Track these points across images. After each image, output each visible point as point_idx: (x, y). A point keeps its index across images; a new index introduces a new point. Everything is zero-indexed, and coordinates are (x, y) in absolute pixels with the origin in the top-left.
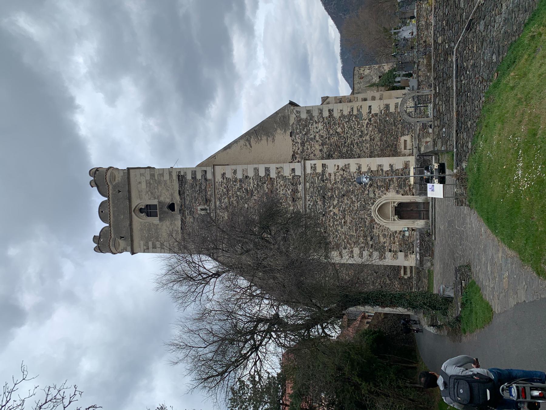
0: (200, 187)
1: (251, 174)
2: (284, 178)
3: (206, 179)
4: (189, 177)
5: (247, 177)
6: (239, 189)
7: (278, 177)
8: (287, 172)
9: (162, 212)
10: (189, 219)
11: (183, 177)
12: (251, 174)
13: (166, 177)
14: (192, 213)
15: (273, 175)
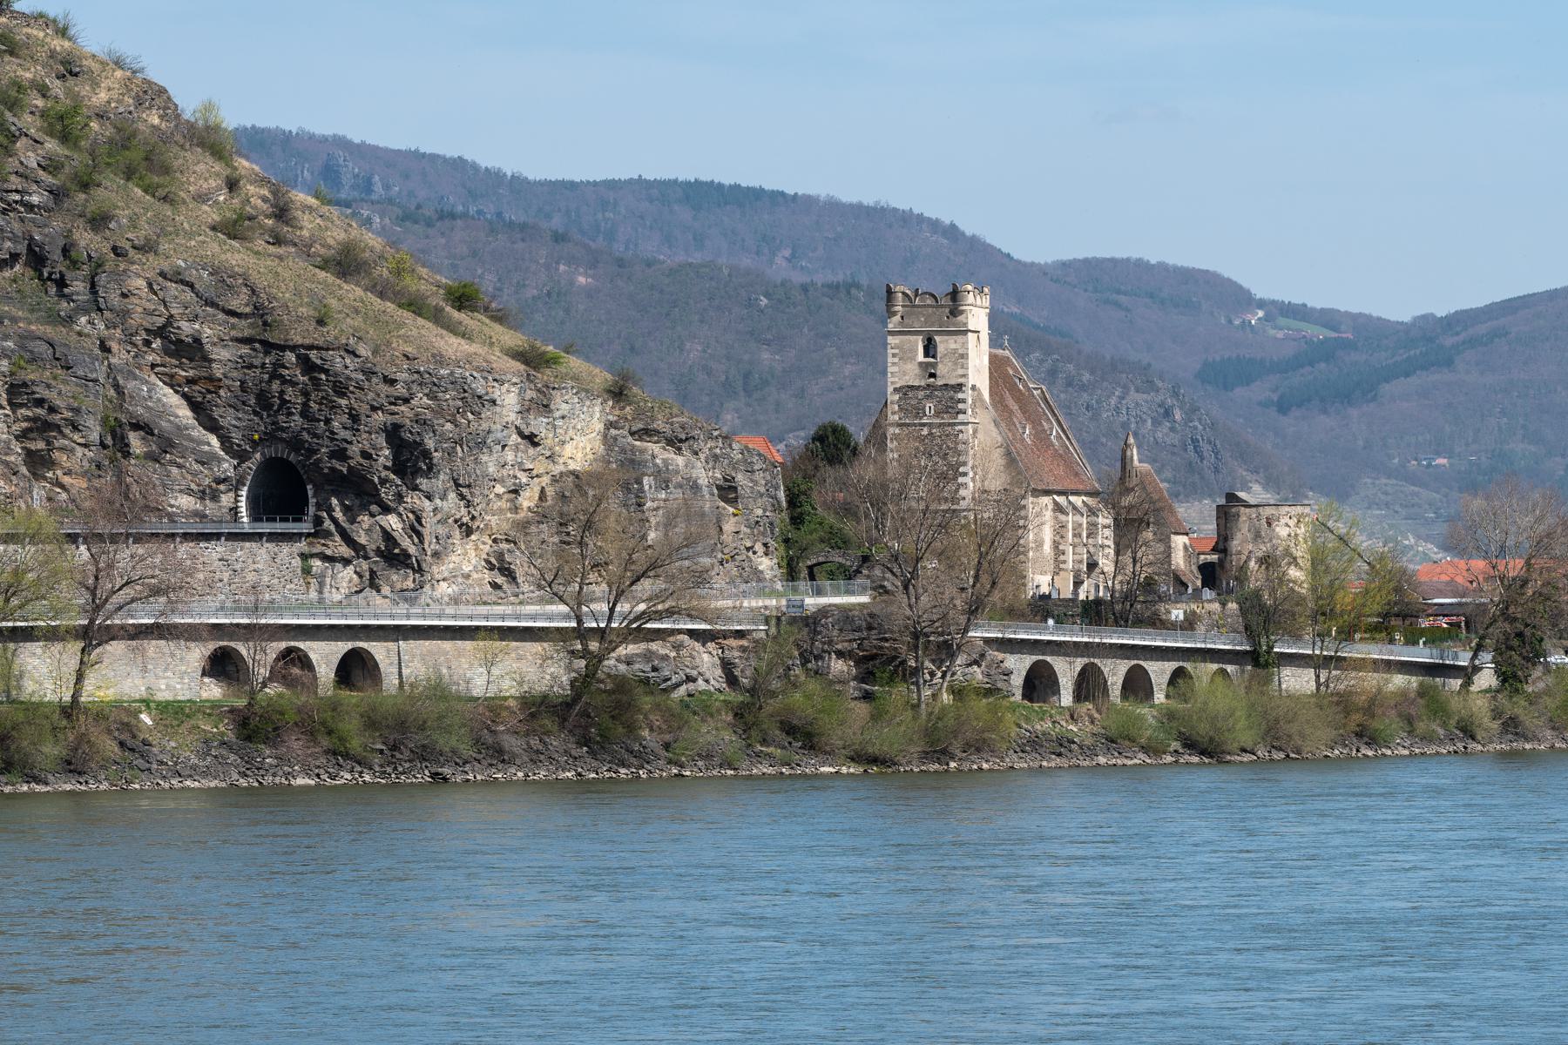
0: (951, 407)
1: (962, 459)
2: (957, 490)
3: (958, 413)
4: (960, 396)
5: (959, 455)
6: (948, 447)
7: (959, 485)
8: (962, 492)
9: (928, 365)
10: (921, 394)
11: (961, 389)
12: (962, 459)
13: (960, 372)
14: (927, 397)
15: (961, 480)
